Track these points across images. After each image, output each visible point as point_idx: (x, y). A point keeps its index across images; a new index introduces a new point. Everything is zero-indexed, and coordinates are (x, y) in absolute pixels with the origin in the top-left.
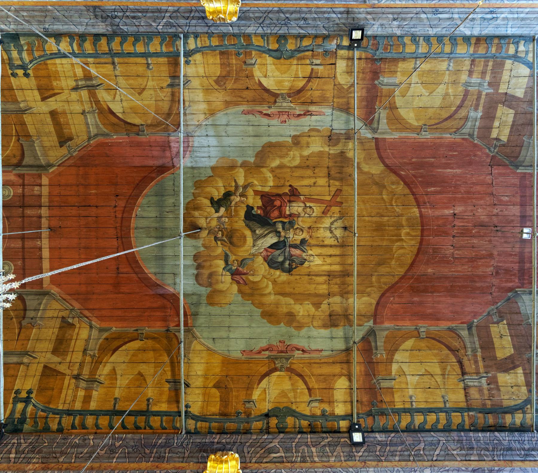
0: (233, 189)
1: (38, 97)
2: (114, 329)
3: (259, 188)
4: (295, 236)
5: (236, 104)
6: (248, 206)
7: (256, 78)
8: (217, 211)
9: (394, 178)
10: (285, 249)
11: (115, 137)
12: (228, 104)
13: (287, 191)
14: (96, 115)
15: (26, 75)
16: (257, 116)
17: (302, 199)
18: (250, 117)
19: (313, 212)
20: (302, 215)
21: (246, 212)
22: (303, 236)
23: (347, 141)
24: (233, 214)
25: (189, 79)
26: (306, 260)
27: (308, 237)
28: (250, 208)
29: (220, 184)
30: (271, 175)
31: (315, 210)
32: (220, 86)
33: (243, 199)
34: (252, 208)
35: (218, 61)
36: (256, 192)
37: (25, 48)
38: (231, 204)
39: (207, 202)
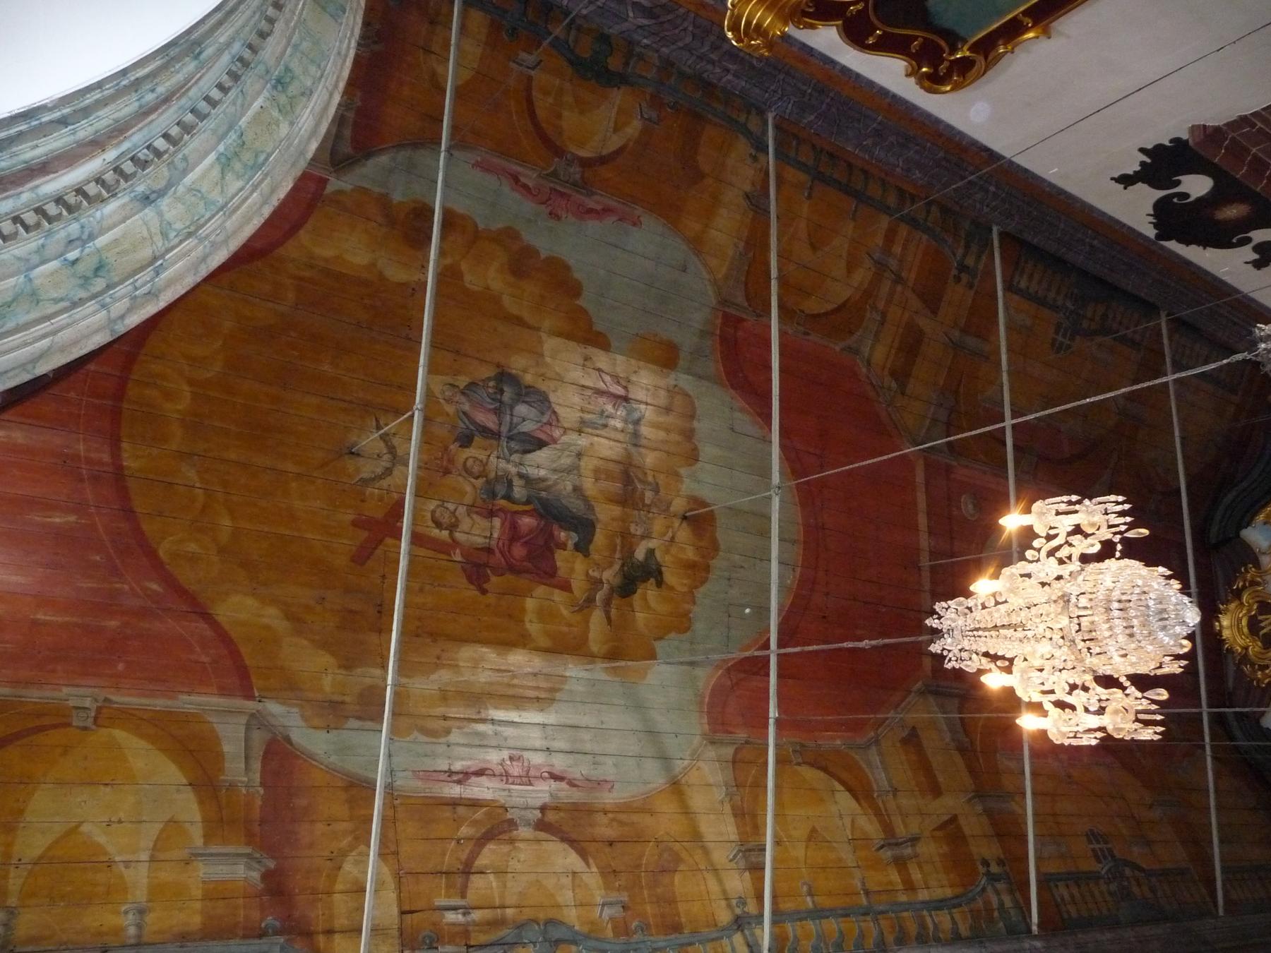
0: (616, 601)
1: (962, 821)
2: (837, 349)
3: (558, 596)
4: (484, 458)
5: (626, 808)
6: (586, 554)
7: (594, 869)
8: (651, 552)
9: (187, 576)
10: (510, 431)
11: (838, 742)
12: (644, 807)
13: (494, 579)
14: (875, 787)
15: (986, 863)
16: (578, 776)
17: (458, 551)
18: (597, 774)
19: (433, 512)
20: (462, 510)
21: (590, 541)
22: (465, 456)
23: (340, 698)
24: (618, 541)
25: (733, 865)
26: (463, 393)
27: (453, 447)
28: (583, 548)
29: (640, 616)
30: (528, 625)
31: (429, 515)
32: (671, 849)
33: (596, 574)
34: (577, 547)
35: (682, 907)
36: (566, 587)
37: (996, 914)
38: (623, 565)
39: (670, 577)
